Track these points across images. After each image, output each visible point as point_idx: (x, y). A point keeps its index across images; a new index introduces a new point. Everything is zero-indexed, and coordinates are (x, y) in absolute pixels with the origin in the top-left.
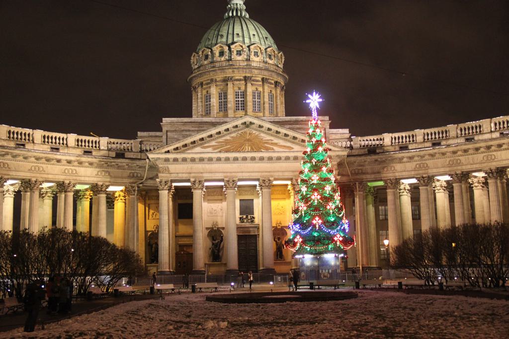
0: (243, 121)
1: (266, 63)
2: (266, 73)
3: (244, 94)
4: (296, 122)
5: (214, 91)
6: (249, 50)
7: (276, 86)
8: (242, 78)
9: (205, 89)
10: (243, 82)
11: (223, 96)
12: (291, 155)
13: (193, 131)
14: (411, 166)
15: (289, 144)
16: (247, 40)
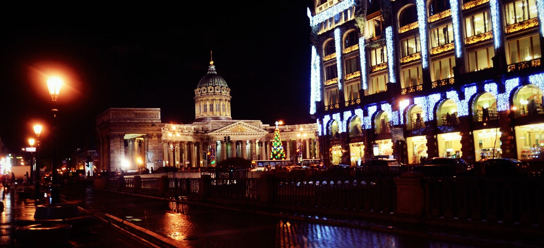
0: (238, 123)
1: (226, 93)
2: (226, 97)
3: (219, 105)
4: (251, 122)
5: (208, 104)
6: (221, 89)
7: (229, 102)
8: (219, 99)
9: (204, 102)
10: (219, 101)
11: (212, 106)
12: (253, 133)
13: (220, 124)
14: (285, 136)
15: (251, 130)
16: (220, 85)
